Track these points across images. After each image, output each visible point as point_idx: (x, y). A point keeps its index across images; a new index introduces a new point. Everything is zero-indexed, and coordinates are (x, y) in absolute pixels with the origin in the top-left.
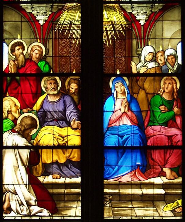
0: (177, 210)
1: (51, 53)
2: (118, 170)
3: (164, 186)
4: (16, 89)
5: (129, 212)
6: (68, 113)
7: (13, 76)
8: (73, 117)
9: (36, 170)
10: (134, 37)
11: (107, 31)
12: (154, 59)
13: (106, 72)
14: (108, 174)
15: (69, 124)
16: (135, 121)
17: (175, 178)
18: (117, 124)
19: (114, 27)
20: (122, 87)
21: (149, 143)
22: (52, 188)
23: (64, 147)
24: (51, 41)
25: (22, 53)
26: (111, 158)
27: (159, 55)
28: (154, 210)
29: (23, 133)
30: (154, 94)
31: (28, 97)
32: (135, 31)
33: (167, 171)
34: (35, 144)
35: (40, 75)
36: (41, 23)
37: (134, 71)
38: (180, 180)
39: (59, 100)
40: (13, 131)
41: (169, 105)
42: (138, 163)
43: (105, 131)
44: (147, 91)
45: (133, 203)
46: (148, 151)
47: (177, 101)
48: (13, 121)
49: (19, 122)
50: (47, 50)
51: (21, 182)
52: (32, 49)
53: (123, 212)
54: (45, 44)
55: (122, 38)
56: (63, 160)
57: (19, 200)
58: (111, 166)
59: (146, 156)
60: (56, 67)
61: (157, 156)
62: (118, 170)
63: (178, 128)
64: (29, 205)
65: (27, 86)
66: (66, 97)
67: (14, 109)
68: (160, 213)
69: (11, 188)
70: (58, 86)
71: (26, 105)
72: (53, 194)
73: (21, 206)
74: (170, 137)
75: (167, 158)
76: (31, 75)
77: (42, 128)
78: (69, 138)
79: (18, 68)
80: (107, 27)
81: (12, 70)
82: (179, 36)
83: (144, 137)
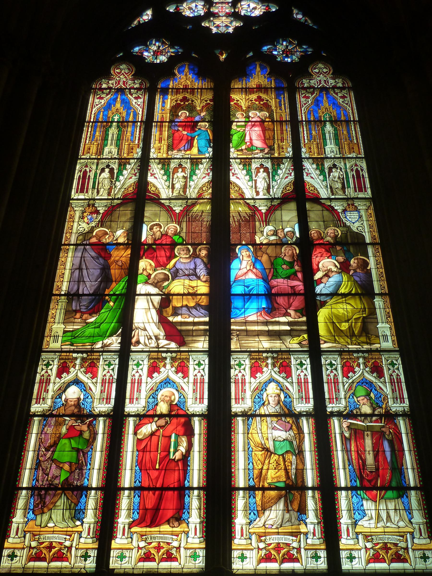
0: (303, 343)
1: (184, 230)
2: (245, 311)
3: (289, 324)
4: (152, 254)
5: (256, 344)
6: (198, 271)
7: (150, 245)
8: (203, 273)
9: (166, 311)
10: (256, 220)
11: (233, 216)
12: (275, 233)
13: (232, 243)
14: (236, 315)
15: (199, 278)
16: (260, 276)
17: (300, 318)
18: (243, 278)
19: (239, 214)
20: (248, 253)
21: (273, 291)
22: (181, 326)
23: (194, 295)
24: (185, 223)
25: (160, 231)
27: (279, 231)
28: (280, 343)
29: (155, 285)
30: (276, 257)
31: (163, 260)
33: (292, 312)
34: (166, 293)
35: (174, 244)
36: (177, 211)
37: (258, 242)
38: (304, 319)
39: (190, 262)
40: (146, 283)
41: (291, 265)
42: (264, 306)
43: (231, 283)
44: (270, 255)
45: (260, 337)
46: (273, 297)
47: (297, 261)
48: (147, 276)
49: (152, 276)
50: (182, 229)
51: (151, 321)
52: (168, 228)
53: (250, 345)
54: (179, 223)
56: (192, 304)
57: (148, 335)
58: (238, 309)
59: (271, 301)
60: (189, 239)
61: (281, 300)
62: (245, 311)
63: (300, 281)
64: (157, 338)
66: (196, 259)
67: (149, 267)
68: (287, 345)
69: (141, 326)
70: (189, 251)
72: (181, 331)
73: (150, 340)
74: (292, 287)
75: (291, 302)
76: (166, 244)
77: (173, 280)
78: (198, 288)
79: (155, 240)
81: (150, 241)
83: (269, 288)
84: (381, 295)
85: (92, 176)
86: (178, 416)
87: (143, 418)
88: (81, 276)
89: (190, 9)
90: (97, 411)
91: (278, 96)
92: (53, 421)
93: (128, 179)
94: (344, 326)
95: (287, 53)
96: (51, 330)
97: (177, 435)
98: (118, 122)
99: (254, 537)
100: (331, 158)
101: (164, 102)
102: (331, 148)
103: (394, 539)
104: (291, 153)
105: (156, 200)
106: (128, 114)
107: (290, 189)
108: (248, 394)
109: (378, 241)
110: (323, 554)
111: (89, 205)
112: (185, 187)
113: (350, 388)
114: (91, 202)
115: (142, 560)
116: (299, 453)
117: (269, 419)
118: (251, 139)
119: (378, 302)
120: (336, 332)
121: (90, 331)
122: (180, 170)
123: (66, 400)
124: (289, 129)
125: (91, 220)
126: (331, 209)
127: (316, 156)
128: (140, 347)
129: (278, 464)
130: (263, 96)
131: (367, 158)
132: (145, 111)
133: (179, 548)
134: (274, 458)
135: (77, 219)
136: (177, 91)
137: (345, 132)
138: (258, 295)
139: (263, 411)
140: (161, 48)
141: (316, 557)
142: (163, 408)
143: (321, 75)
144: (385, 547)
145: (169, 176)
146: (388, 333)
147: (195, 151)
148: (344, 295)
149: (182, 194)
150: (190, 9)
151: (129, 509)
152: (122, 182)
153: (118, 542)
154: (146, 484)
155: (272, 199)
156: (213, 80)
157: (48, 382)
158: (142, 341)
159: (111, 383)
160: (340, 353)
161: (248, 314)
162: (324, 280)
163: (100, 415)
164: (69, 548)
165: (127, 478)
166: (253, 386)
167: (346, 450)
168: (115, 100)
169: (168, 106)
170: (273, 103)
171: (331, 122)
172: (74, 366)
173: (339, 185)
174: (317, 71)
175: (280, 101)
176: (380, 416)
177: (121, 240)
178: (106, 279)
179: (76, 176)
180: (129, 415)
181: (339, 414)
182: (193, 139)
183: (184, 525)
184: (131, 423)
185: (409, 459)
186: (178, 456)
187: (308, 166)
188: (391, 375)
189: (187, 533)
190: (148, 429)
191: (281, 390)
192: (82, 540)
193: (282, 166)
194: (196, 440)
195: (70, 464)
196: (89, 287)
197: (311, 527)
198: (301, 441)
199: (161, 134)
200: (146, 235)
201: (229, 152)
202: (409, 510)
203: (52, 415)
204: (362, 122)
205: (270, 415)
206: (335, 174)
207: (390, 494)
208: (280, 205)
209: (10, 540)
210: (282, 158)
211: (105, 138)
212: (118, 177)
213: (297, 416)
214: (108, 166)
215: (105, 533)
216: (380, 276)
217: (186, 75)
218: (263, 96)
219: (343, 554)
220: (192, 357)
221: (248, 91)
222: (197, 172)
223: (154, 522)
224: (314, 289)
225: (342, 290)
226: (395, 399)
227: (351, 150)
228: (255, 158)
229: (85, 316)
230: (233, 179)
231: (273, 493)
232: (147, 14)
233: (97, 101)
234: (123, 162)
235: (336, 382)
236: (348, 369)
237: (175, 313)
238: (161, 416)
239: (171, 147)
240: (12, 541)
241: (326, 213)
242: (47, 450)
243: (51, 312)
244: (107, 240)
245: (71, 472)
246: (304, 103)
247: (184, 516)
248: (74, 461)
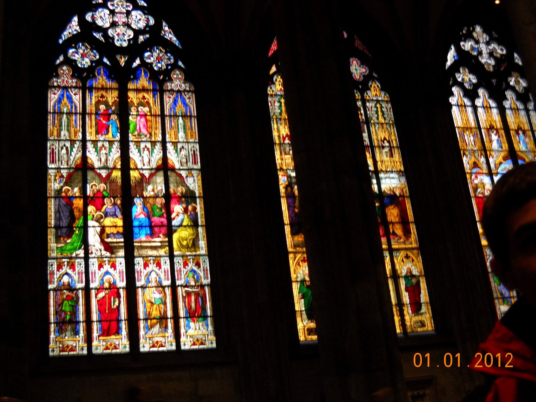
3: (160, 242)
6: (117, 213)
12: (153, 190)
15: (117, 217)
23: (116, 226)
26: (136, 230)
29: (98, 221)
32: (144, 180)
33: (161, 235)
35: (104, 197)
36: (104, 176)
37: (145, 196)
40: (92, 220)
41: (161, 209)
49: (95, 216)
50: (107, 188)
54: (106, 184)
55: (139, 183)
56: (115, 232)
64: (101, 250)
65: (99, 201)
67: (93, 211)
71: (98, 209)
72: (111, 247)
74: (162, 222)
76: (100, 197)
79: (94, 194)
80: (132, 178)
81: (92, 195)
82: (163, 182)
84: (202, 226)
85: (57, 153)
86: (113, 289)
87: (99, 290)
88: (60, 217)
89: (101, 17)
90: (78, 287)
91: (154, 96)
92: (59, 293)
93: (76, 155)
94: (185, 243)
95: (159, 59)
96: (50, 247)
97: (114, 298)
98: (67, 113)
99: (148, 339)
100: (181, 142)
101: (91, 98)
102: (181, 134)
103: (201, 337)
104: (161, 138)
105: (93, 169)
106: (72, 107)
107: (160, 162)
108: (143, 277)
109: (202, 195)
110: (174, 344)
111: (58, 172)
112: (106, 160)
113: (186, 273)
114: (59, 170)
115: (104, 349)
116: (165, 303)
117: (152, 289)
118: (140, 128)
119: (200, 230)
120: (181, 246)
121: (69, 247)
122: (103, 148)
123: (64, 283)
124: (160, 121)
125: (60, 182)
126: (180, 176)
127: (174, 140)
128: (93, 255)
129: (156, 309)
130: (146, 95)
131: (200, 143)
132: (81, 104)
133: (119, 345)
134: (155, 306)
135: (53, 181)
136: (98, 89)
137: (189, 124)
138: (145, 227)
139: (150, 285)
140: (86, 52)
141: (172, 345)
142: (106, 285)
143: (178, 82)
144: (198, 340)
145: (98, 153)
146: (204, 246)
147: (110, 134)
148: (185, 226)
149: (105, 164)
150: (101, 17)
151: (97, 330)
152: (74, 156)
153: (95, 343)
154: (103, 319)
155: (151, 169)
156: (118, 82)
157: (53, 274)
158: (94, 252)
159: (82, 273)
160: (183, 256)
161: (141, 237)
162: (176, 218)
163: (79, 289)
164: (76, 347)
165: (95, 317)
166: (145, 274)
167: (184, 302)
168: (63, 95)
169: (94, 102)
170: (151, 101)
171: (182, 116)
172: (64, 265)
173: (184, 160)
174: (175, 76)
175: (155, 101)
176: (198, 286)
177: (77, 195)
178: (73, 219)
179: (49, 151)
180: (92, 289)
181: (181, 286)
182: (109, 126)
183: (120, 335)
184: (93, 292)
185: (208, 305)
186: (115, 307)
187: (169, 146)
188: (204, 267)
189: (122, 339)
190: (101, 295)
191: (157, 275)
192: (80, 343)
193: (156, 147)
194: (122, 299)
195: (70, 312)
196: (64, 223)
197: (169, 334)
198: (166, 298)
199: (91, 122)
200: (89, 192)
201: (128, 136)
202: (207, 325)
203: (58, 290)
204: (198, 117)
205: (152, 287)
206: (183, 152)
207: (200, 319)
208: (155, 173)
209: (51, 344)
210: (156, 142)
211: (60, 125)
212: (71, 153)
213: (163, 287)
214: (65, 145)
215: (89, 340)
216: (202, 215)
217: (102, 77)
218: (146, 95)
219: (182, 344)
220: (118, 259)
221: (137, 91)
222: (112, 150)
223: (108, 335)
224: (171, 223)
225: (185, 223)
226: (205, 278)
227: (192, 136)
228: (142, 141)
229: (65, 239)
230: (131, 155)
231: (155, 321)
232: (75, 21)
233: (53, 96)
234: (73, 142)
235: (180, 270)
236: (185, 264)
237: (108, 236)
238: (106, 289)
239: (97, 133)
240: (52, 345)
241: (178, 178)
242: (59, 306)
243: (49, 237)
244: (70, 194)
245: (71, 315)
246: (168, 100)
247: (120, 332)
248: (71, 310)
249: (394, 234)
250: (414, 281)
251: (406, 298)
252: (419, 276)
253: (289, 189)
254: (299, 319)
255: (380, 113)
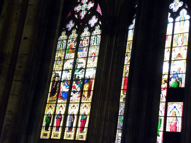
249: (84, 96)
250: (85, 117)
251: (79, 125)
252: (87, 115)
253: (54, 78)
254: (42, 129)
255: (95, 41)
